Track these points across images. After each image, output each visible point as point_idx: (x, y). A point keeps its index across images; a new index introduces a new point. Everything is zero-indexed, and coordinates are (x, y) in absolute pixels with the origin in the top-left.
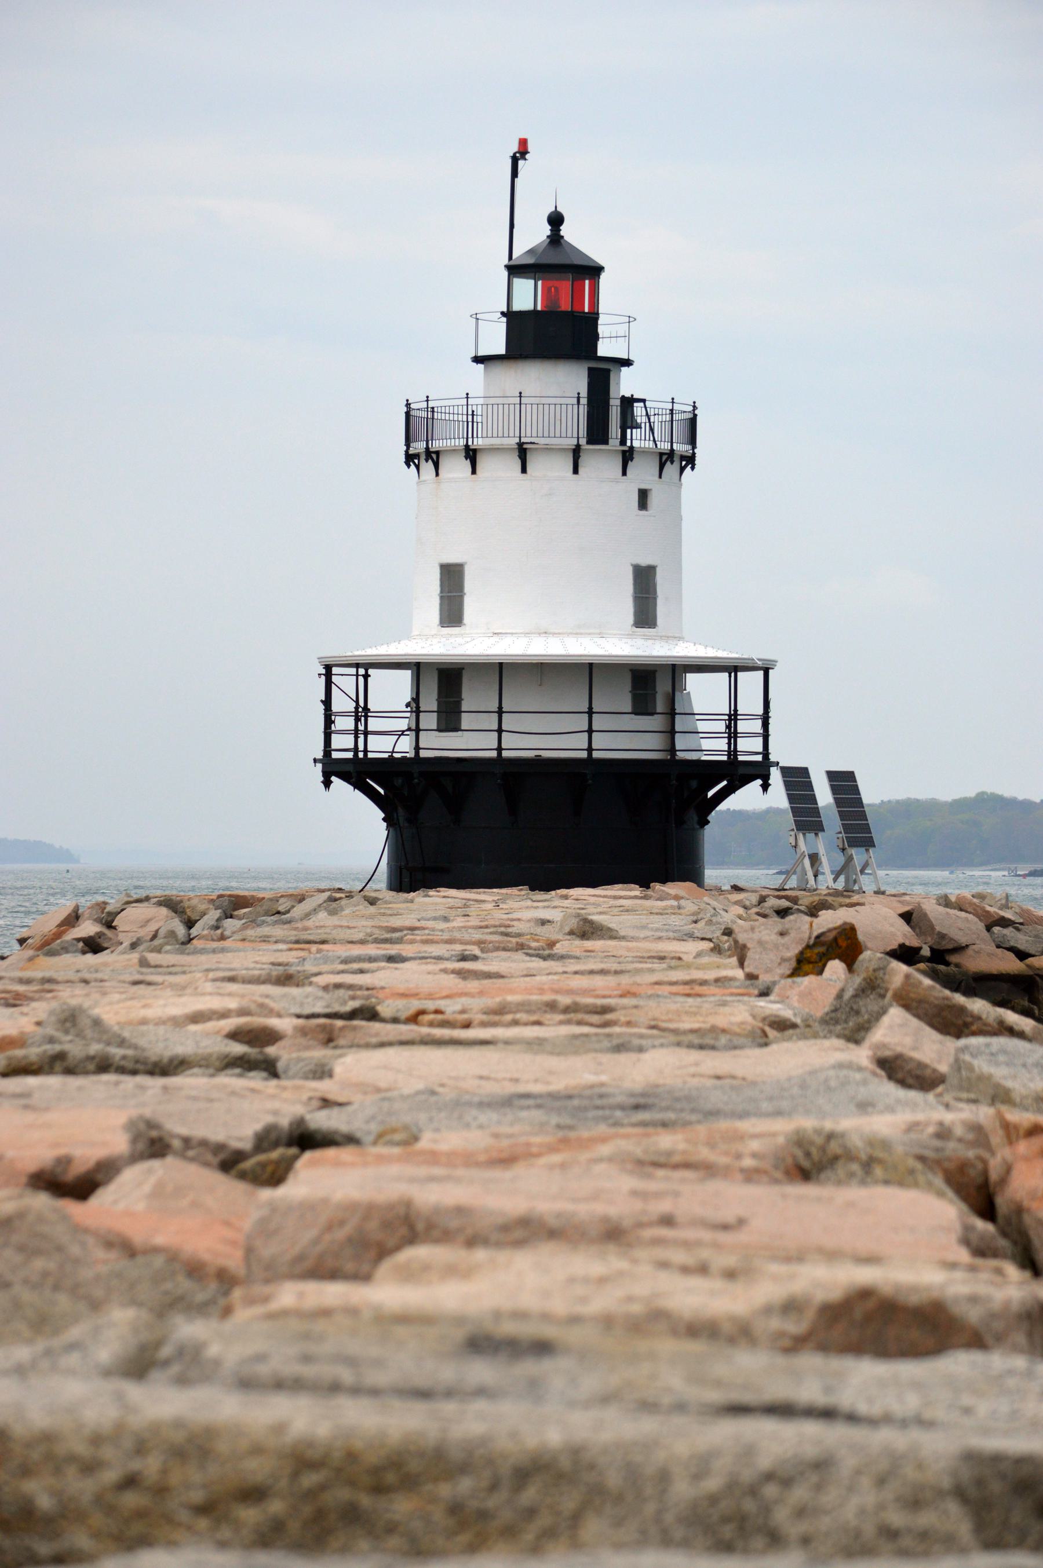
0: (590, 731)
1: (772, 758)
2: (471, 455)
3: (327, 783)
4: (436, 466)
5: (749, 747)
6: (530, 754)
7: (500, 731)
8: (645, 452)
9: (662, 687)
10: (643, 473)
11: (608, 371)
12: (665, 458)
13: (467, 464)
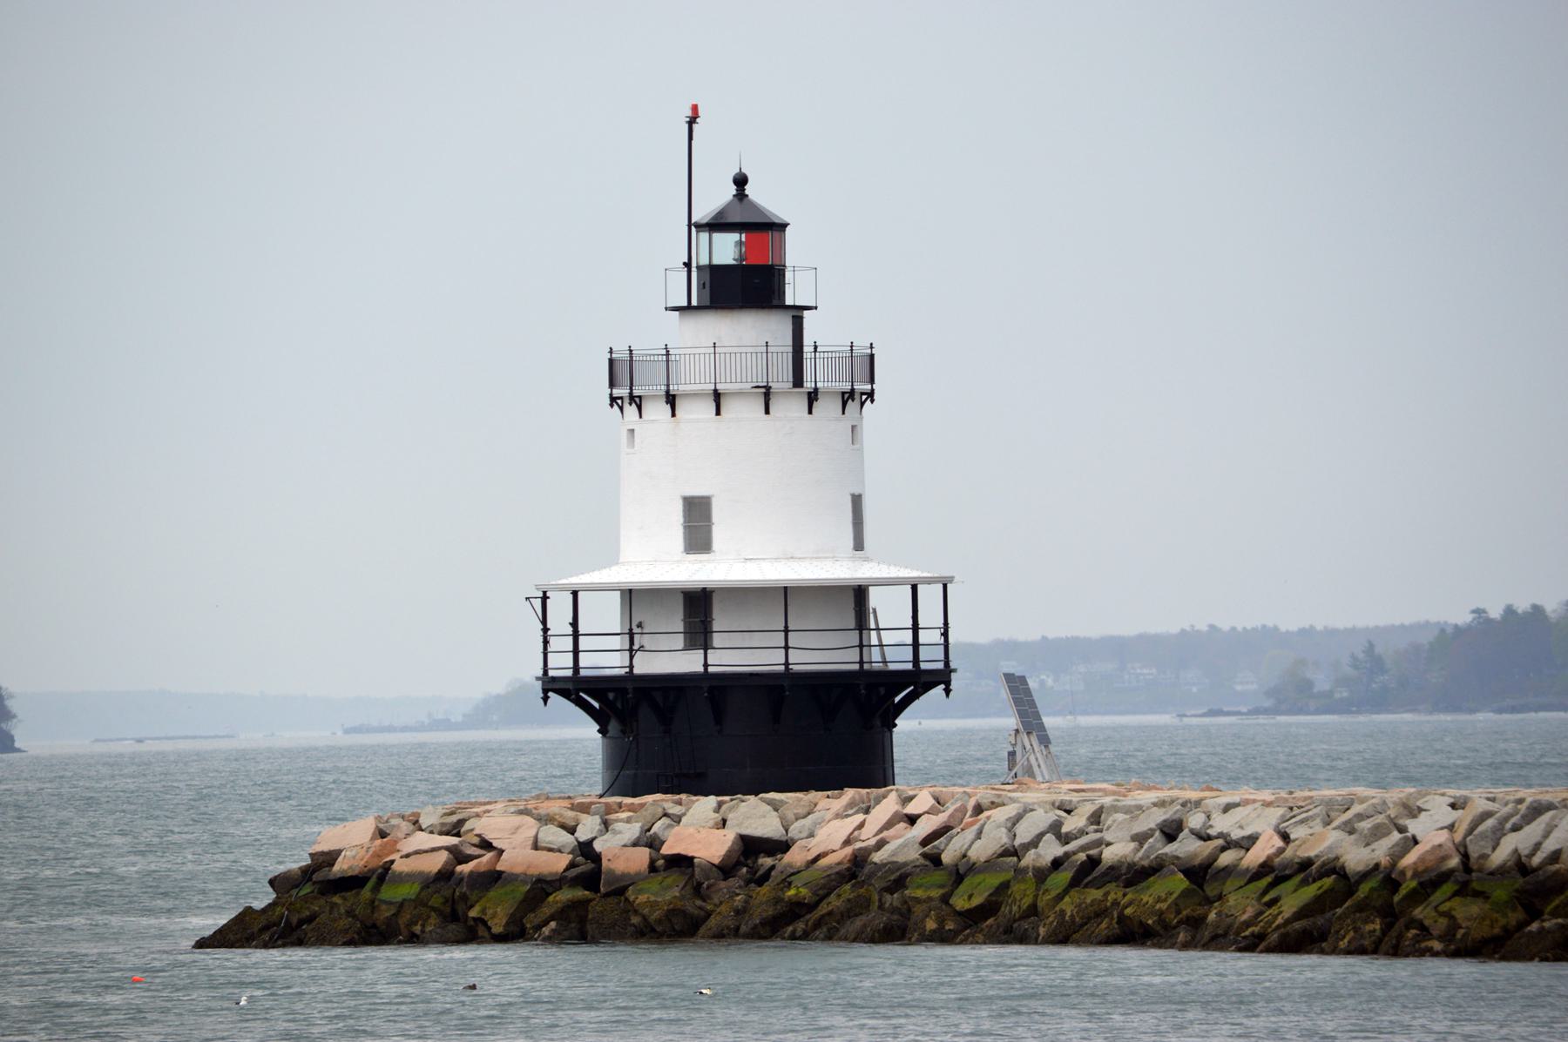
1: (953, 665)
2: (671, 400)
3: (546, 699)
4: (639, 408)
5: (931, 659)
8: (830, 393)
12: (847, 397)
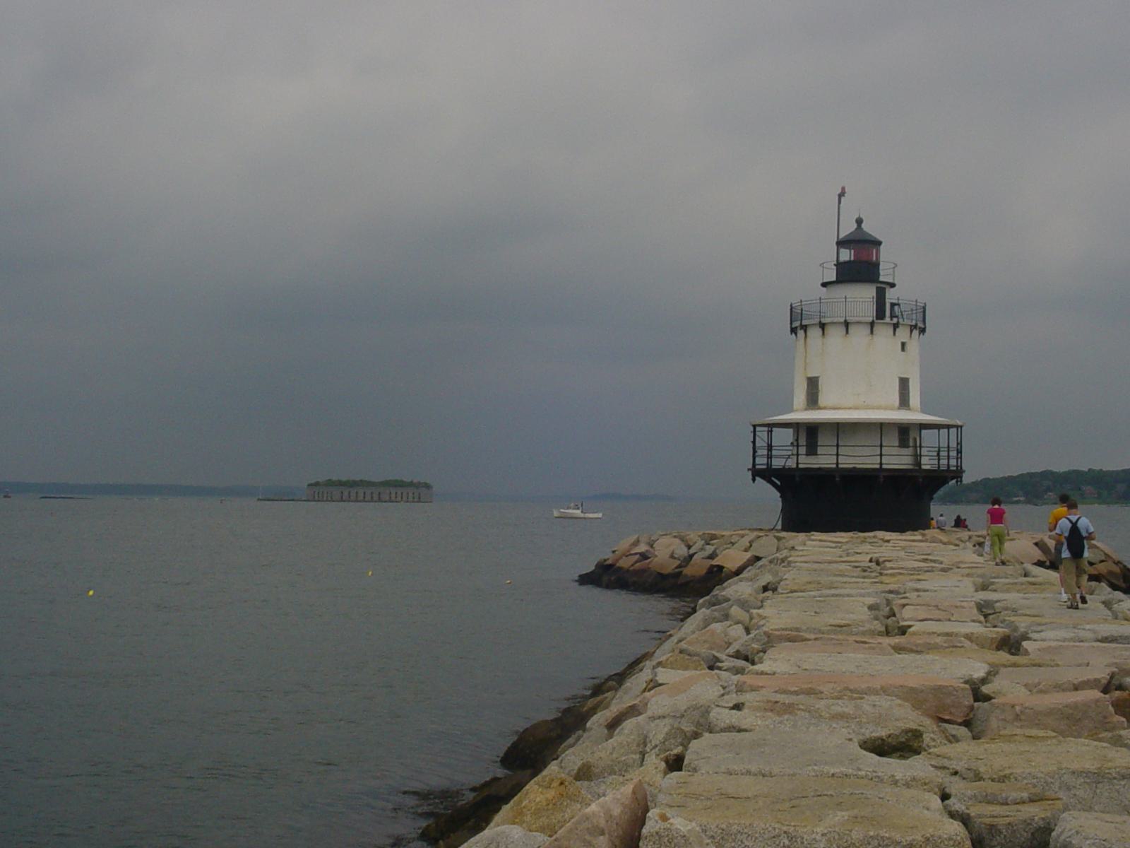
0: (881, 455)
2: (822, 326)
3: (754, 480)
4: (805, 332)
6: (851, 466)
7: (837, 455)
9: (913, 434)
10: (903, 333)
11: (885, 289)
13: (820, 330)
